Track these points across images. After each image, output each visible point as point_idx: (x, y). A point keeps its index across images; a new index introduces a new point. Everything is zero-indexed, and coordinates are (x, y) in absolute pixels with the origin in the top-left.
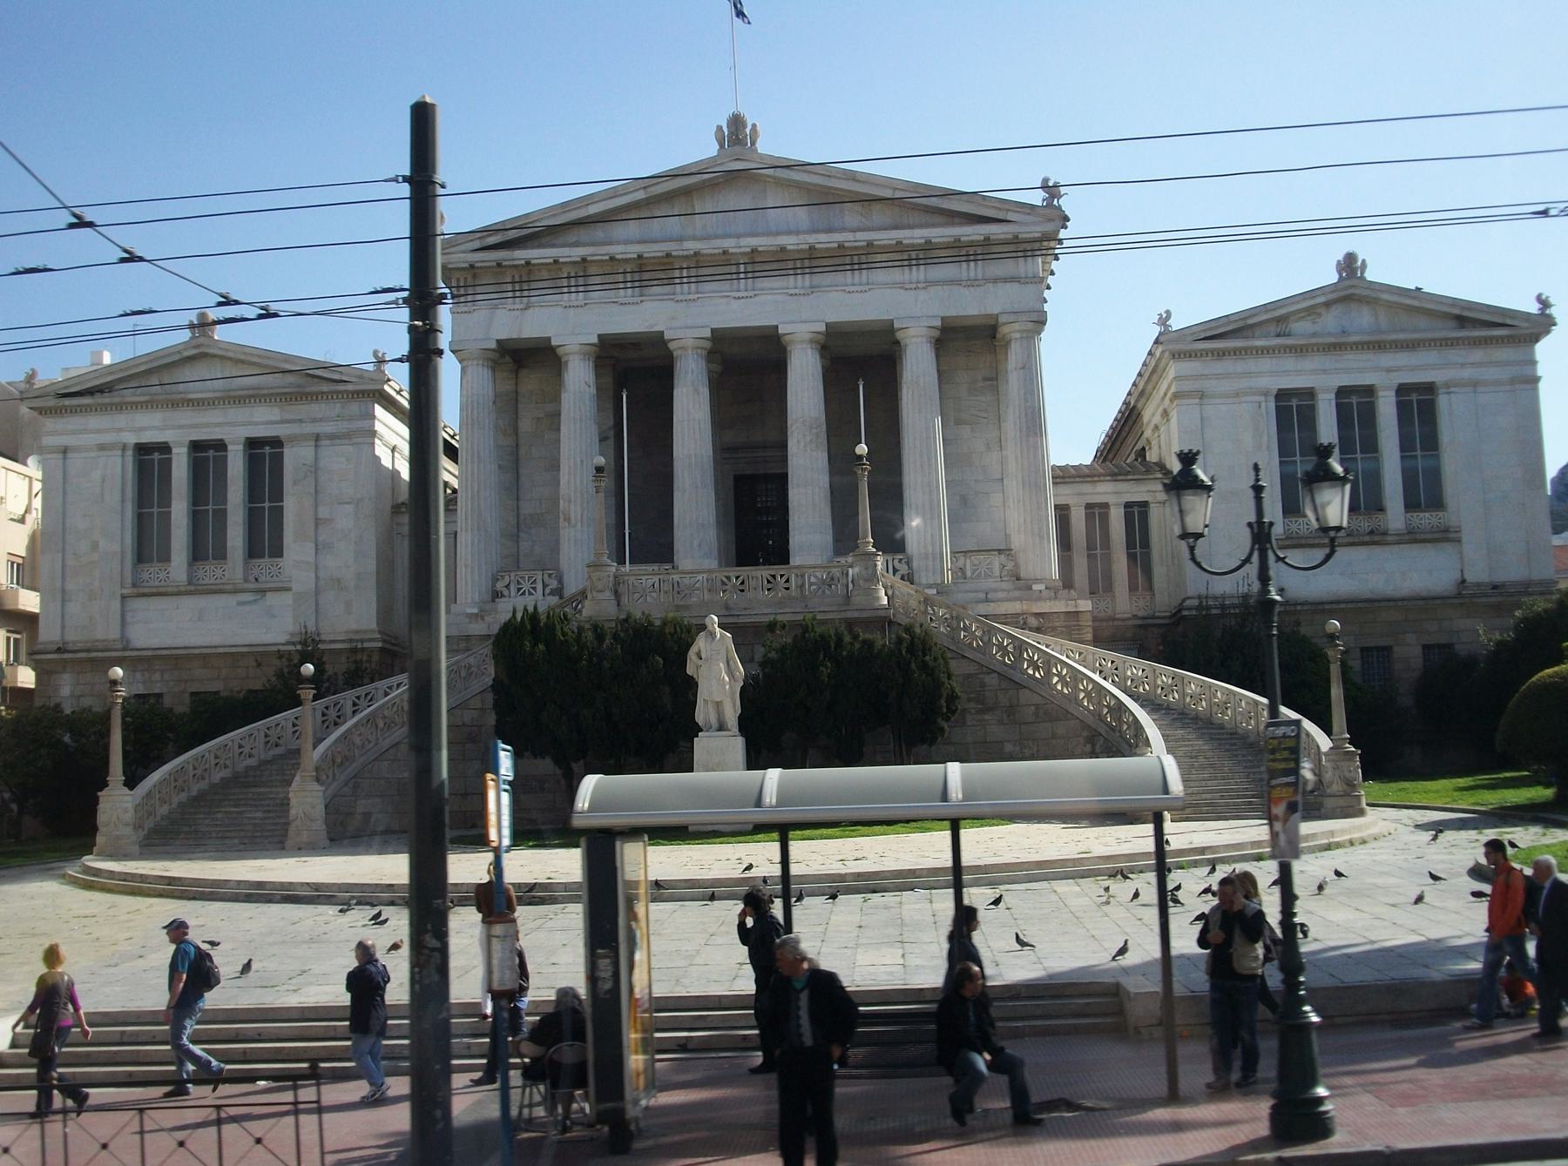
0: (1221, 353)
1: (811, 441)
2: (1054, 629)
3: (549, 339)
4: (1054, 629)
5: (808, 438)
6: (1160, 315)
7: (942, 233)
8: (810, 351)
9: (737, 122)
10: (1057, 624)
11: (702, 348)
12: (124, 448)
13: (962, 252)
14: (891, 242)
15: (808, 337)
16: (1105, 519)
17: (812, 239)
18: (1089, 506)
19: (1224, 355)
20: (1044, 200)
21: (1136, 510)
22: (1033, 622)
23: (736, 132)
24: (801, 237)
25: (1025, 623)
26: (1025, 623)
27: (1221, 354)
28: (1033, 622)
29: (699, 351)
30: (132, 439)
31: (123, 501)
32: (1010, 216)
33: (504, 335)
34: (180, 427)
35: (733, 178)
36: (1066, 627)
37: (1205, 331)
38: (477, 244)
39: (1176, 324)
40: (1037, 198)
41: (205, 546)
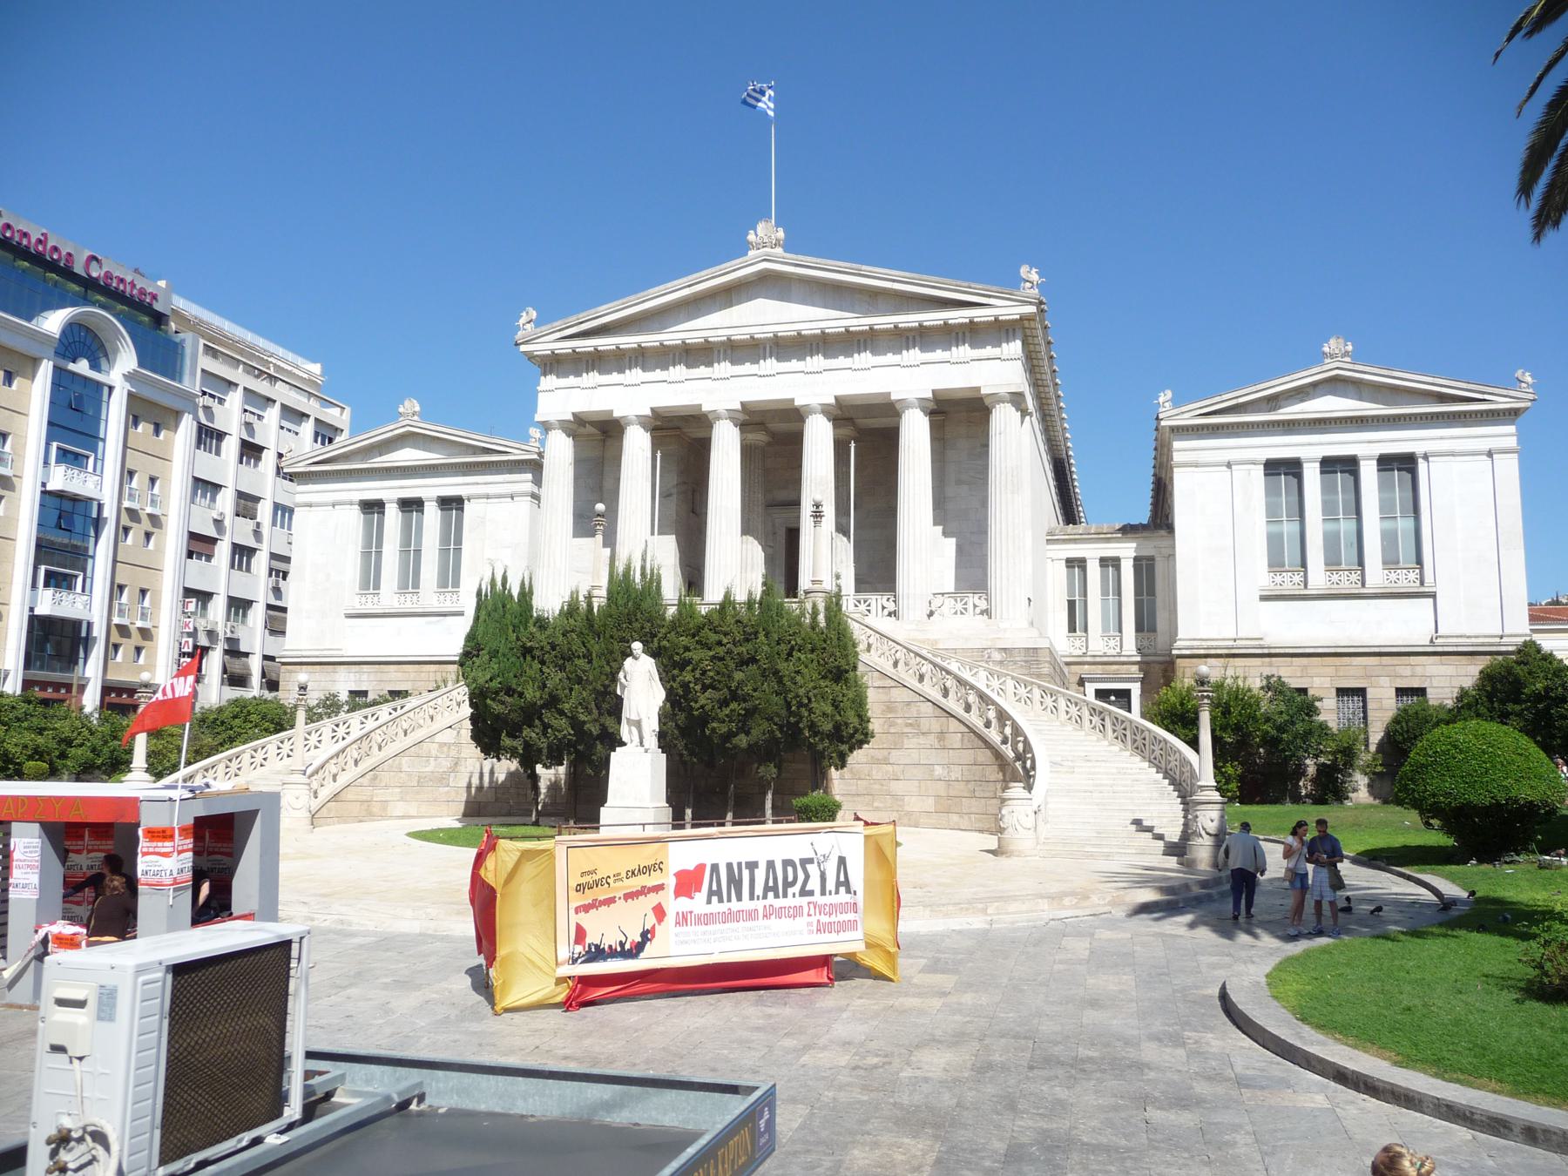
2: (1015, 663)
3: (612, 411)
4: (1015, 663)
14: (889, 326)
21: (1144, 562)
22: (997, 656)
26: (989, 657)
28: (997, 656)
36: (1026, 662)
38: (558, 335)
41: (410, 579)
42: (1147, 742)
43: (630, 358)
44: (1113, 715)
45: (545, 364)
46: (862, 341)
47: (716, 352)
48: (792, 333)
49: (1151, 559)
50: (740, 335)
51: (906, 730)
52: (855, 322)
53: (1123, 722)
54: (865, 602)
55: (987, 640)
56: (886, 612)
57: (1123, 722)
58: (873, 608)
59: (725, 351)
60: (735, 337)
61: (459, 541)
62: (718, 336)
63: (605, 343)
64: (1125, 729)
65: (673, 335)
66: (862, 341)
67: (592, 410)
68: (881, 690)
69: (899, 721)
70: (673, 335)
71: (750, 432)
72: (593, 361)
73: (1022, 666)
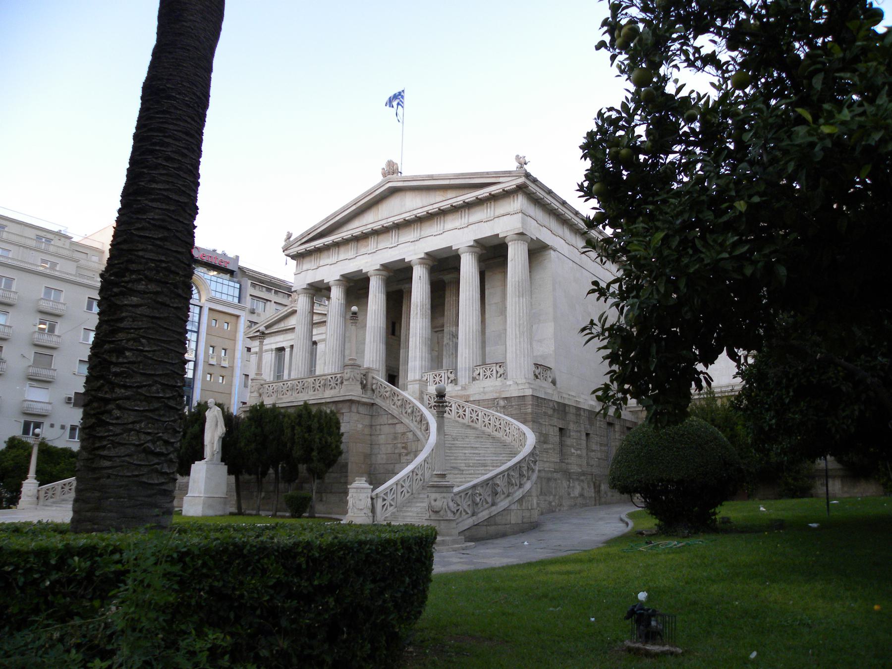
7: (470, 196)
9: (391, 164)
10: (513, 404)
11: (382, 275)
12: (272, 350)
13: (479, 202)
17: (415, 212)
20: (517, 168)
22: (502, 403)
23: (391, 169)
26: (498, 404)
28: (502, 403)
30: (274, 346)
31: (271, 371)
32: (501, 180)
34: (287, 340)
35: (394, 191)
36: (518, 405)
38: (299, 243)
40: (513, 166)
48: (401, 220)
50: (376, 226)
54: (439, 375)
55: (496, 392)
56: (450, 381)
58: (443, 379)
61: (315, 367)
62: (367, 229)
63: (319, 243)
67: (316, 280)
68: (391, 426)
73: (516, 409)
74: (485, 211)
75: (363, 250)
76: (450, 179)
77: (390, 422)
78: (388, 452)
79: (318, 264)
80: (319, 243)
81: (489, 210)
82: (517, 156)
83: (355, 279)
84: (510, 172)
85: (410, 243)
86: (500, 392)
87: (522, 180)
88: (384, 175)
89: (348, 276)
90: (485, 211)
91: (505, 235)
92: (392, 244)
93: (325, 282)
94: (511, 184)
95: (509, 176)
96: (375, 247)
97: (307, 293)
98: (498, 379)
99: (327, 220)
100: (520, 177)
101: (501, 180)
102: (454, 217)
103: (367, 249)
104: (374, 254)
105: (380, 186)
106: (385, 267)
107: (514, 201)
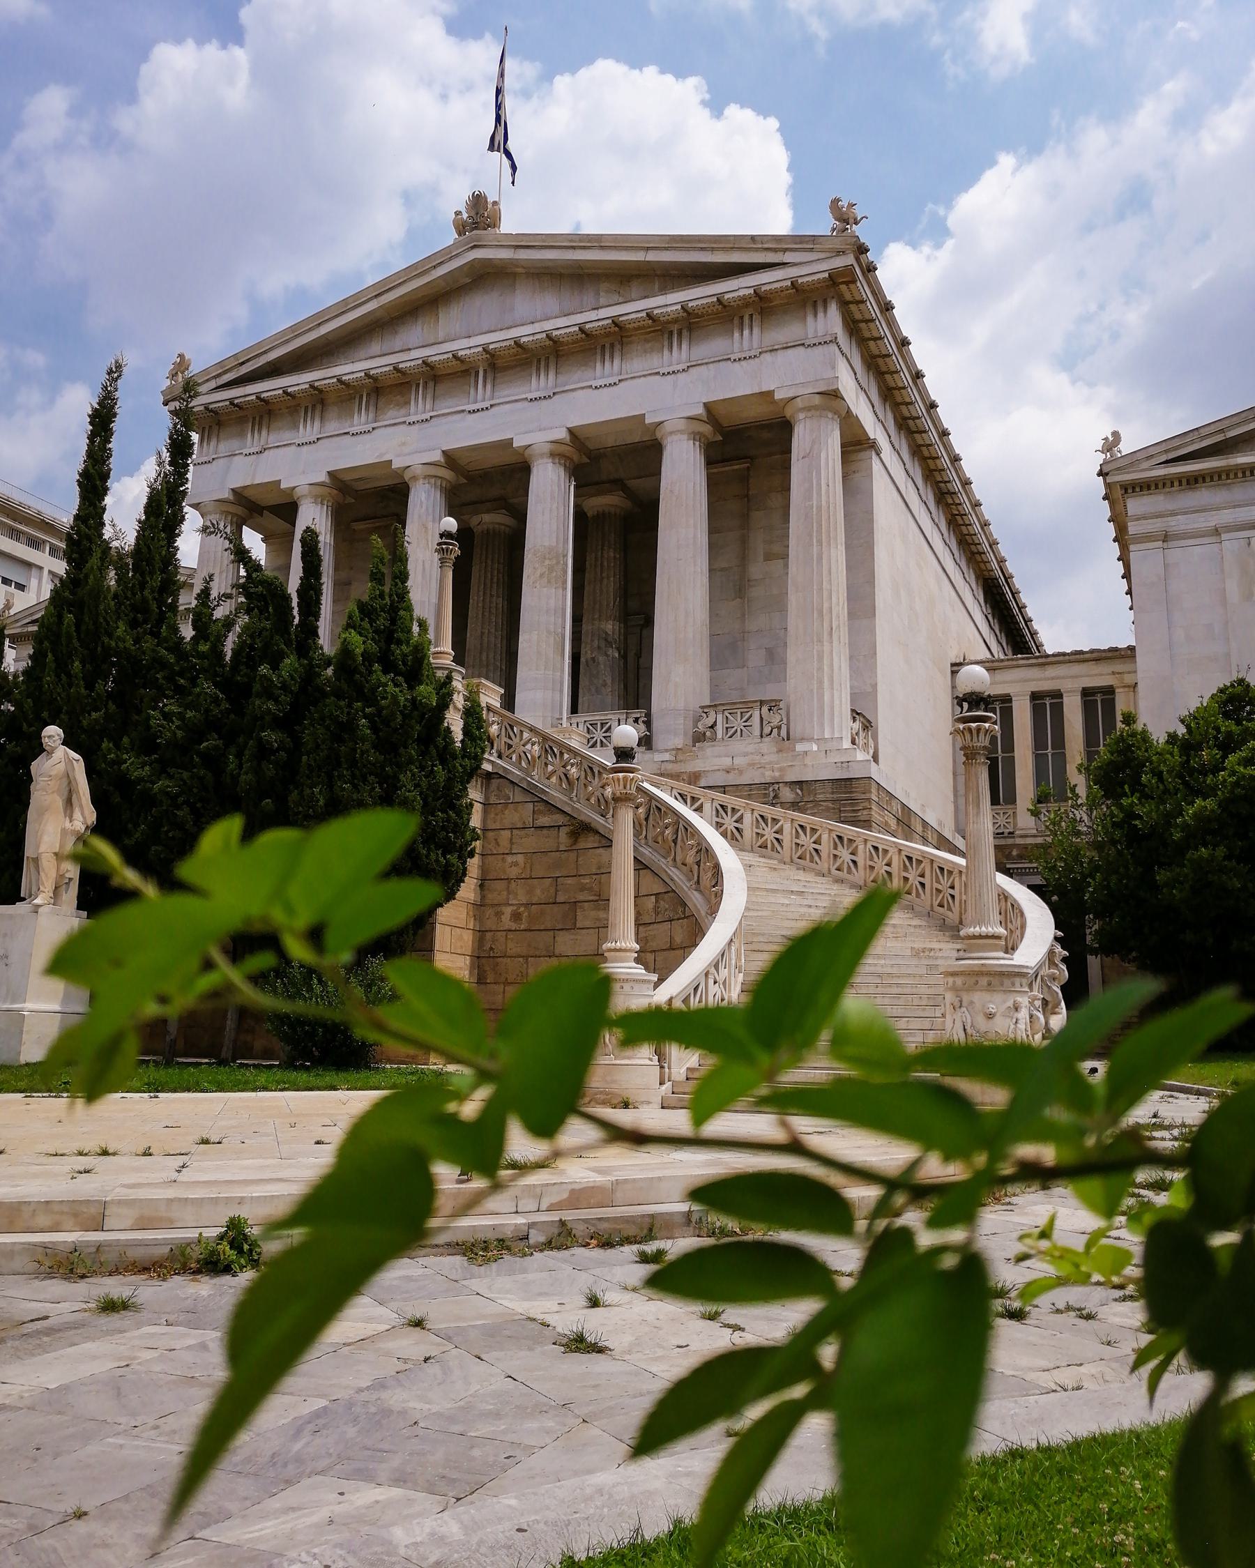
0: (1192, 481)
1: (542, 576)
2: (816, 803)
4: (816, 803)
5: (538, 572)
6: (1106, 439)
8: (550, 466)
10: (821, 797)
15: (547, 448)
16: (1058, 709)
17: (548, 325)
18: (1035, 696)
19: (1196, 481)
20: (833, 230)
21: (1099, 698)
22: (787, 794)
24: (536, 325)
25: (776, 797)
26: (776, 797)
27: (1193, 481)
28: (787, 794)
29: (433, 481)
32: (788, 258)
33: (237, 484)
36: (833, 801)
37: (1166, 451)
39: (1127, 447)
42: (927, 881)
43: (306, 408)
44: (935, 866)
45: (204, 428)
46: (607, 346)
47: (414, 388)
49: (1109, 691)
51: (581, 898)
52: (593, 315)
53: (919, 862)
57: (919, 862)
59: (426, 383)
60: (433, 359)
63: (270, 387)
64: (922, 876)
65: (351, 368)
66: (607, 346)
67: (258, 480)
69: (569, 881)
70: (351, 368)
71: (488, 511)
72: (261, 417)
73: (828, 809)
74: (737, 335)
75: (392, 415)
76: (648, 249)
77: (544, 820)
78: (535, 900)
79: (262, 442)
80: (270, 387)
81: (746, 332)
82: (835, 202)
83: (361, 486)
84: (814, 238)
85: (526, 404)
86: (781, 769)
87: (849, 260)
88: (461, 228)
89: (347, 477)
90: (737, 335)
91: (791, 395)
92: (476, 402)
93: (283, 486)
94: (812, 269)
95: (811, 250)
96: (428, 407)
97: (228, 513)
98: (766, 739)
99: (296, 331)
100: (840, 253)
101: (788, 258)
102: (648, 346)
103: (403, 411)
104: (425, 425)
105: (446, 255)
106: (450, 459)
107: (815, 315)
